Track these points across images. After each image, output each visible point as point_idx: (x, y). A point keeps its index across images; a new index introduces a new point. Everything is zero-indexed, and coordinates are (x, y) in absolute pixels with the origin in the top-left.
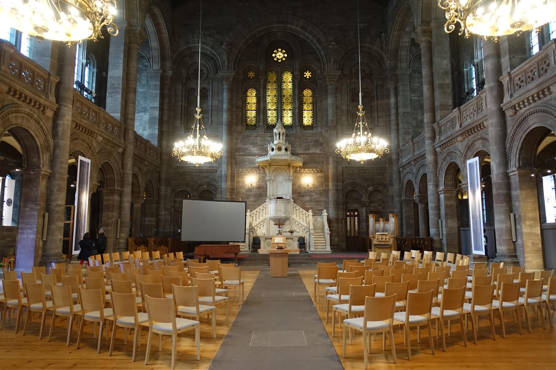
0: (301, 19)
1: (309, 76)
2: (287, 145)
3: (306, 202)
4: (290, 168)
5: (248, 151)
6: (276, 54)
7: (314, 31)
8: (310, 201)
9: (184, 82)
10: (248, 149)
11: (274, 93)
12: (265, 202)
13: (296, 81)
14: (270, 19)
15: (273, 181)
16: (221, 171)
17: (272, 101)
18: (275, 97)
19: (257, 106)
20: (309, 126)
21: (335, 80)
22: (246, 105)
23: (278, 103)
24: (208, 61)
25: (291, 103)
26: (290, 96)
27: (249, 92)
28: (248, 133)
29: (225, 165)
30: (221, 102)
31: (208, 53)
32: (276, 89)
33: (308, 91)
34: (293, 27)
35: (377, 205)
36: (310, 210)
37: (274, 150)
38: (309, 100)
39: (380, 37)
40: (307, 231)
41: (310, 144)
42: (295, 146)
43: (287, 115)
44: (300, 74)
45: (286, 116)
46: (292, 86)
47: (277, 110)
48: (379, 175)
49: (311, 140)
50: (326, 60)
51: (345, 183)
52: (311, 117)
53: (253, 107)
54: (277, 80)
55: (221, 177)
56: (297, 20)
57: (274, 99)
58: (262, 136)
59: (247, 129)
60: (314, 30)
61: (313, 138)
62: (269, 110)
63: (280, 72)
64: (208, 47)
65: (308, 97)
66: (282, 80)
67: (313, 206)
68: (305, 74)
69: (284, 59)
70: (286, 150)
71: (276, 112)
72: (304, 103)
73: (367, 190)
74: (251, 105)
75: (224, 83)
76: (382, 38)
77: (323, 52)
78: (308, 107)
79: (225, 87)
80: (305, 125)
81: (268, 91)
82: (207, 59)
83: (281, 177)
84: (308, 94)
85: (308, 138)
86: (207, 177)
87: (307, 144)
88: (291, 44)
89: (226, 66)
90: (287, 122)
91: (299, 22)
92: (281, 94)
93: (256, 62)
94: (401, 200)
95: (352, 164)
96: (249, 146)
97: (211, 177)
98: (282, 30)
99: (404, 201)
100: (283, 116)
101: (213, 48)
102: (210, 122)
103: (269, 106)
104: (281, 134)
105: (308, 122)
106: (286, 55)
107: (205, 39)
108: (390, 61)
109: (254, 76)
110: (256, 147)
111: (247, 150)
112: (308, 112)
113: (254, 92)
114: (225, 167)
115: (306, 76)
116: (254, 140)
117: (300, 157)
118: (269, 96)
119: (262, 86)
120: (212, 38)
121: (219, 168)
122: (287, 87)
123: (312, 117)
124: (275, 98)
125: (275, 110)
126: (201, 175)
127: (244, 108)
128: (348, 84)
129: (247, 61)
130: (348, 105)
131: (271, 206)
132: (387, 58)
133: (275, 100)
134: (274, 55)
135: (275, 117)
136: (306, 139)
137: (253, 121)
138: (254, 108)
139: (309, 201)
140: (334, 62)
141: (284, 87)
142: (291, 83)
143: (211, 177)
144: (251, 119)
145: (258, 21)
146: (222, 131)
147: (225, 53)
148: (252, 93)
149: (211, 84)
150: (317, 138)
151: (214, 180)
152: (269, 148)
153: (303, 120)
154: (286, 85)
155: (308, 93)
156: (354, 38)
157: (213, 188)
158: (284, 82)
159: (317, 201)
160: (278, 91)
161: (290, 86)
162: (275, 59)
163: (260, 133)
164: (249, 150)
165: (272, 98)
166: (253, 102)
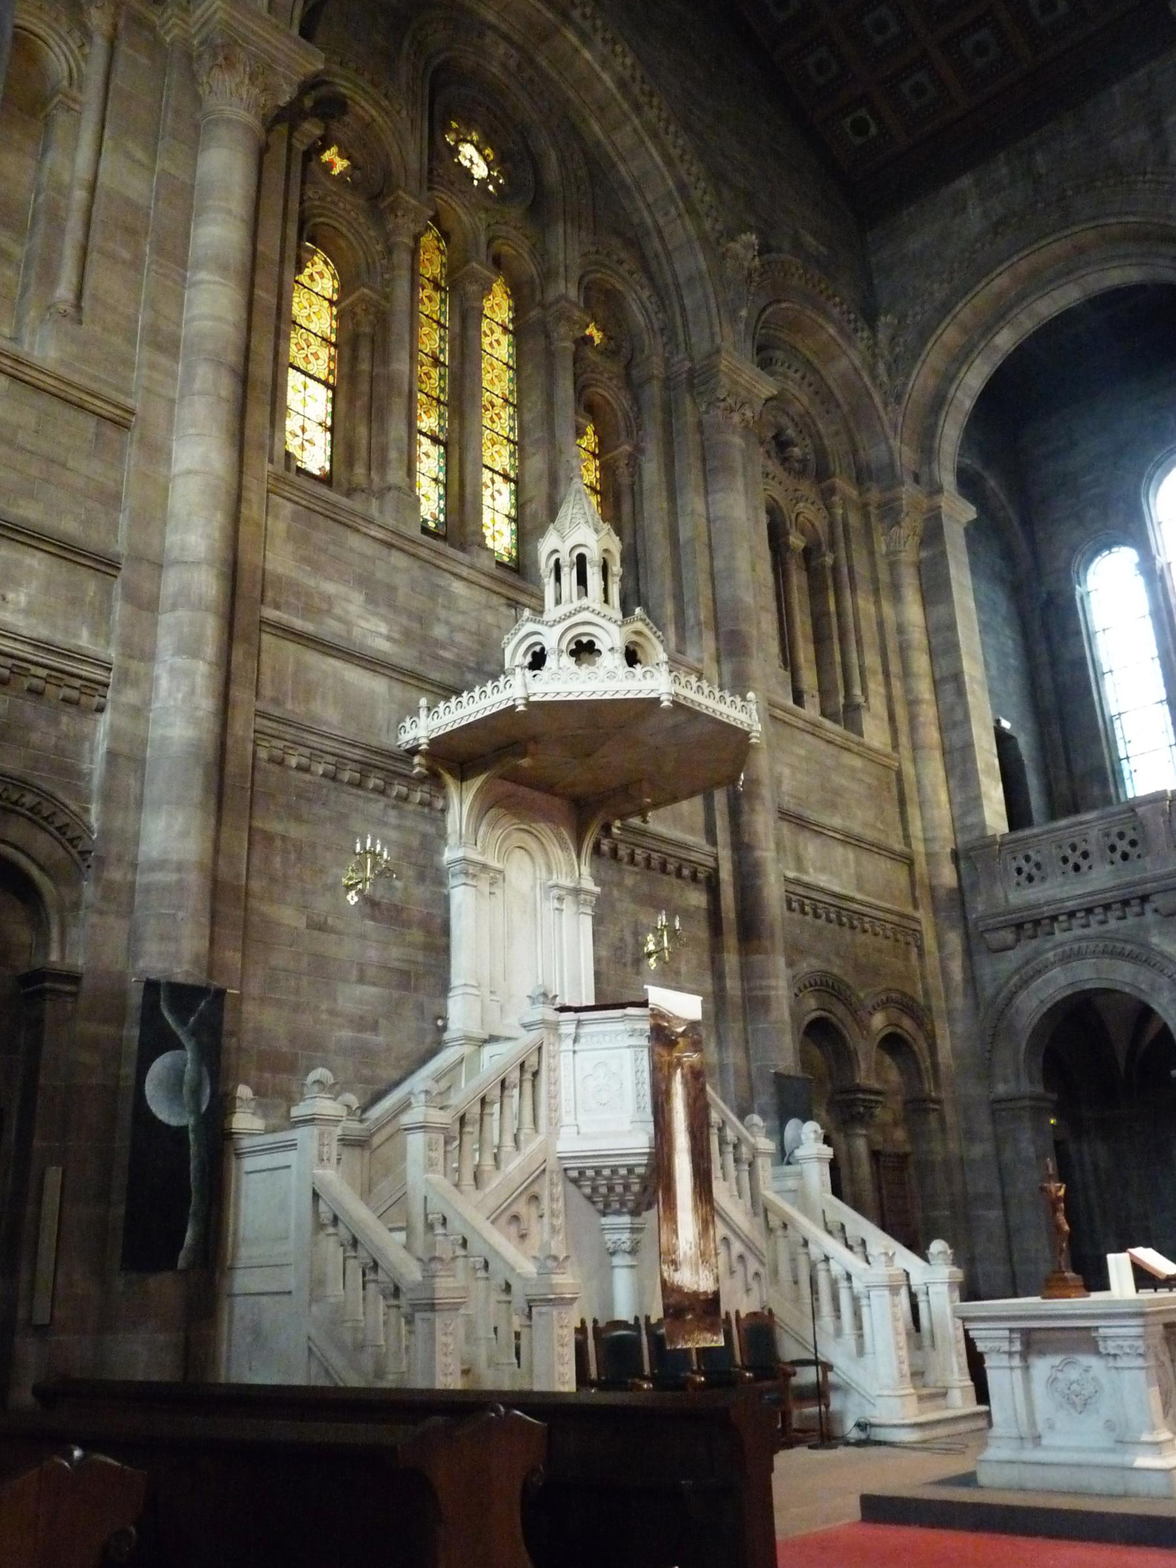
4: (482, 819)
10: (337, 610)
21: (749, 414)
37: (550, 662)
47: (445, 445)
94: (992, 1096)
95: (811, 870)
99: (1027, 1103)
110: (383, 610)
113: (327, 274)
121: (126, 678)
124: (435, 373)
138: (321, 365)
151: (71, 774)
157: (43, 843)
164: (339, 619)
166: (312, 327)
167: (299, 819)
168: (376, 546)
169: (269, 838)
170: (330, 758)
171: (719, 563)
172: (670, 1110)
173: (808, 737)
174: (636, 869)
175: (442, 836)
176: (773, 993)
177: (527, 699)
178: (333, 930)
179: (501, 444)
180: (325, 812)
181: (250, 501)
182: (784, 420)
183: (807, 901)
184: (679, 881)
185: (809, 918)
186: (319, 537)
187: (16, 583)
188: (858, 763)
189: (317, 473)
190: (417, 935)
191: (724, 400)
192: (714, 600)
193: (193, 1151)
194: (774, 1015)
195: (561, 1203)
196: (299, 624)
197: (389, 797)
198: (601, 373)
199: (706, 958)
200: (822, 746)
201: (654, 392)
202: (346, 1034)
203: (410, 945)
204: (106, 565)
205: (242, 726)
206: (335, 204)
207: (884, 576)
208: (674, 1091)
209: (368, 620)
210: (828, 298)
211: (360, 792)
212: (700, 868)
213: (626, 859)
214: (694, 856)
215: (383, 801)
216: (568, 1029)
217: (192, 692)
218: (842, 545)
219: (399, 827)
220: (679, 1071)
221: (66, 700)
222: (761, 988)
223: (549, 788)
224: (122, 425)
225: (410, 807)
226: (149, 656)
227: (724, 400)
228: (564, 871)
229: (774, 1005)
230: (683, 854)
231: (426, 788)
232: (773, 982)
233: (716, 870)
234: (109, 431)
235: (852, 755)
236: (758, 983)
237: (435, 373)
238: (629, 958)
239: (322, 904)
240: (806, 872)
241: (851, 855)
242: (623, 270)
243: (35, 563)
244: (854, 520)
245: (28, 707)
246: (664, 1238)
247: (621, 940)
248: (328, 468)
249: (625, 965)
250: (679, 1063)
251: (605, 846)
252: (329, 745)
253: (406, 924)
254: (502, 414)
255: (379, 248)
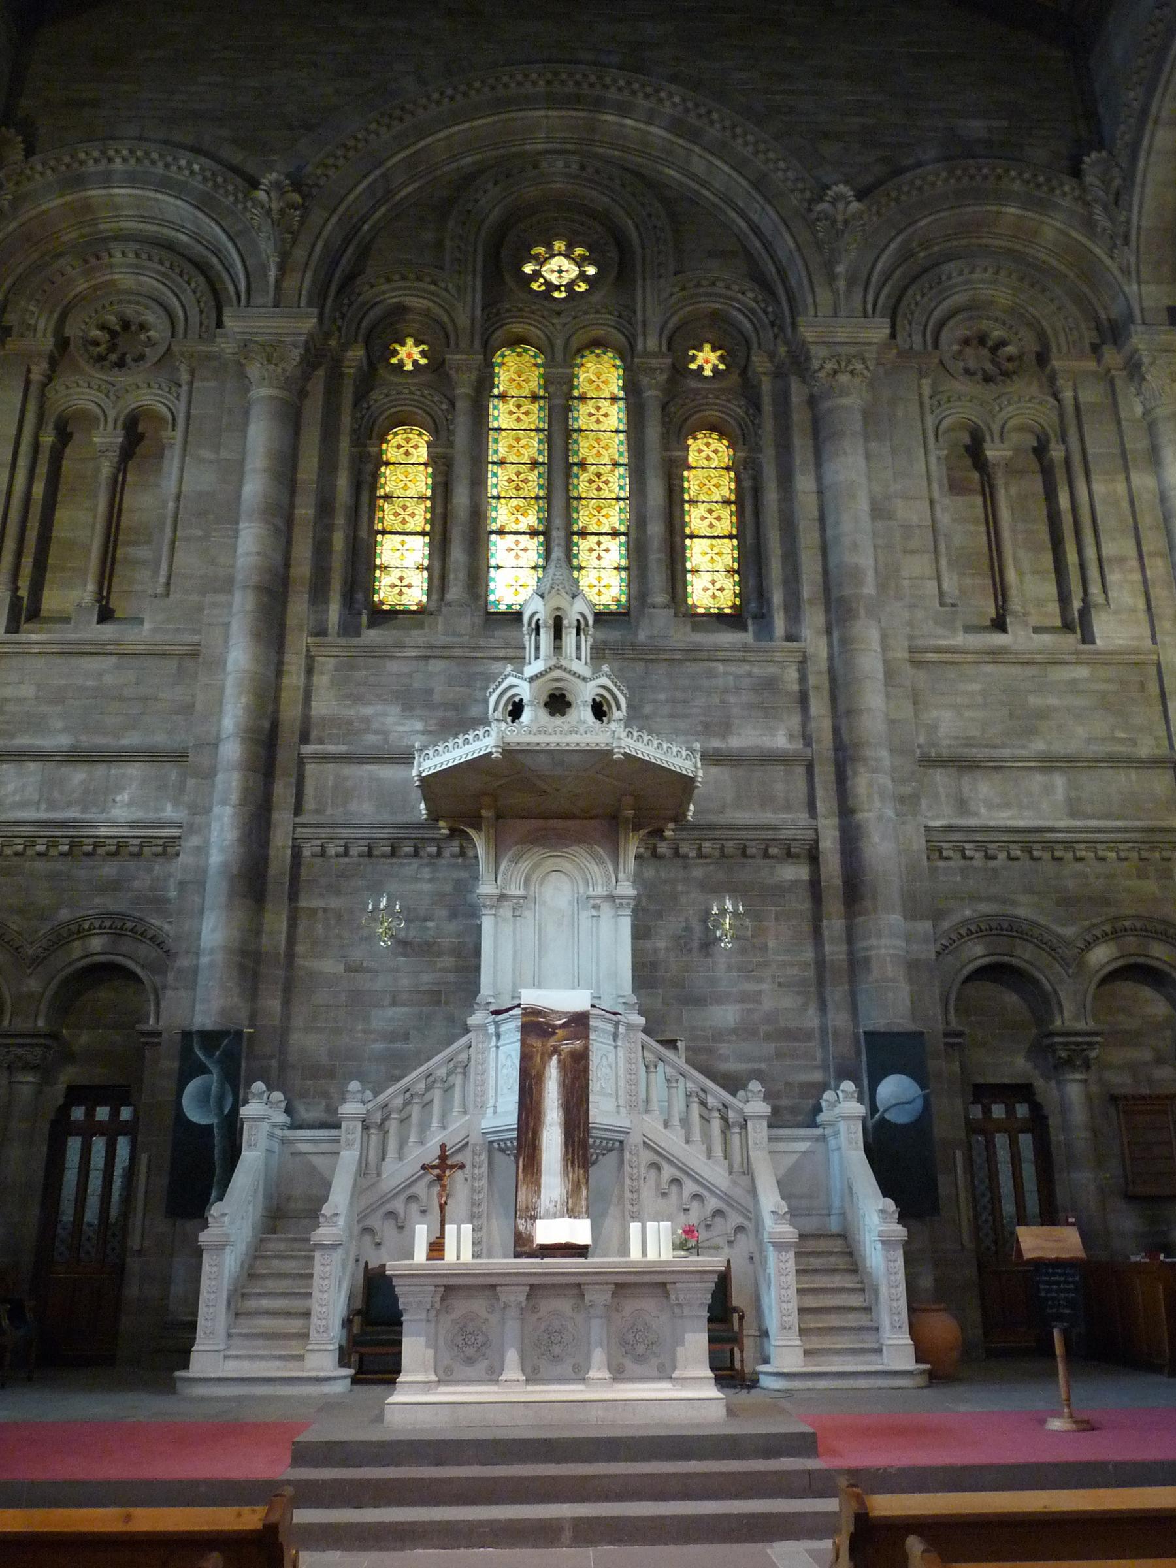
0: (673, 87)
1: (715, 369)
2: (604, 681)
3: (718, 1036)
5: (371, 739)
6: (542, 264)
7: (740, 141)
8: (746, 1031)
9: (36, 376)
10: (375, 726)
11: (532, 447)
12: (467, 1030)
13: (645, 380)
14: (513, 85)
15: (518, 907)
16: (202, 850)
17: (518, 488)
18: (532, 470)
19: (432, 510)
20: (720, 617)
22: (372, 509)
23: (548, 498)
24: (181, 275)
25: (618, 499)
26: (615, 464)
27: (394, 442)
28: (372, 636)
29: (228, 810)
30: (235, 471)
31: (184, 238)
32: (537, 430)
33: (708, 445)
34: (629, 122)
35: (1147, 1055)
36: (755, 1086)
38: (717, 486)
39: (1076, 173)
40: (740, 1229)
41: (732, 699)
42: (648, 709)
43: (599, 558)
44: (669, 349)
45: (596, 563)
46: (622, 415)
48: (1142, 875)
49: (737, 677)
50: (807, 269)
51: (946, 925)
52: (730, 572)
53: (412, 515)
54: (546, 387)
55: (202, 884)
56: (649, 90)
57: (525, 481)
58: (457, 652)
59: (372, 624)
60: (734, 136)
61: (746, 667)
62: (501, 532)
63: (559, 343)
64: (179, 202)
65: (713, 473)
66: (572, 387)
67: (763, 1066)
68: (694, 358)
69: (582, 287)
70: (599, 710)
71: (540, 544)
72: (690, 502)
73: (1081, 964)
74: (405, 508)
75: (254, 370)
76: (1089, 179)
77: (787, 236)
78: (710, 519)
79: (261, 392)
80: (701, 611)
81: (496, 441)
82: (171, 268)
83: (566, 886)
84: (708, 458)
85: (720, 667)
86: (114, 886)
87: (716, 700)
88: (622, 213)
89: (272, 289)
90: (599, 593)
91: (661, 101)
92: (567, 457)
93: (432, 288)
95: (983, 811)
96: (379, 707)
97: (136, 884)
98: (569, 147)
100: (575, 562)
101: (205, 204)
102: (162, 580)
103: (501, 515)
104: (565, 622)
105: (714, 597)
106: (591, 271)
107: (167, 166)
108: (1139, 283)
109: (423, 361)
110: (419, 712)
111: (367, 730)
112: (712, 547)
114: (226, 820)
115: (701, 368)
116: (410, 675)
117: (684, 753)
118: (501, 463)
119: (462, 405)
120: (203, 160)
121: (192, 829)
122: (598, 421)
123: (737, 572)
124: (533, 476)
125: (533, 533)
126: (82, 873)
127: (365, 518)
128: (927, 401)
129: (388, 280)
130: (932, 502)
131: (502, 1056)
132: (1126, 272)
133: (534, 483)
134: (528, 269)
135: (535, 568)
136: (711, 674)
137: (409, 586)
138: (419, 517)
139: (735, 1031)
140: (851, 282)
141: (582, 423)
142: (621, 404)
143: (136, 884)
144: (401, 579)
145: (449, 92)
146: (227, 625)
147: (267, 227)
148: (408, 447)
149: (185, 388)
150: (773, 670)
151: (159, 903)
152: (492, 701)
153: (685, 583)
154: (591, 415)
155: (708, 452)
156: (944, 174)
157: (145, 950)
158: (583, 398)
159: (789, 1035)
160: (550, 439)
161: (615, 416)
162: (534, 286)
163: (442, 640)
164: (377, 733)
165: (518, 474)
166: (409, 493)
167: (338, 893)
168: (415, 662)
169: (313, 912)
170: (362, 842)
171: (830, 533)
172: (540, 1092)
173: (989, 668)
174: (708, 861)
175: (476, 878)
176: (873, 953)
177: (419, 776)
178: (368, 970)
179: (610, 506)
180: (360, 883)
181: (289, 672)
182: (985, 325)
183: (967, 846)
184: (769, 861)
185: (979, 860)
186: (360, 675)
187: (120, 788)
188: (1083, 672)
189: (415, 608)
190: (448, 961)
191: (822, 368)
192: (826, 572)
193: (217, 1140)
194: (875, 974)
195: (484, 1169)
196: (332, 749)
197: (422, 858)
198: (706, 397)
199: (806, 926)
200: (1014, 670)
201: (766, 386)
202: (379, 1046)
203: (444, 970)
204: (179, 756)
205: (281, 840)
206: (399, 393)
207: (1137, 443)
208: (547, 1074)
209: (403, 724)
210: (999, 178)
211: (395, 861)
212: (793, 844)
213: (692, 854)
214: (783, 834)
215: (415, 863)
216: (491, 1029)
217: (222, 830)
218: (1072, 432)
219: (431, 880)
220: (555, 1058)
221: (156, 855)
222: (864, 948)
223: (587, 816)
224: (194, 655)
225: (444, 861)
226: (207, 810)
227: (822, 368)
228: (600, 881)
229: (874, 965)
230: (770, 835)
231: (456, 843)
232: (873, 942)
233: (817, 841)
234: (188, 663)
235: (1072, 667)
236: (865, 944)
237: (533, 476)
238: (695, 944)
239: (357, 954)
240: (976, 814)
241: (1059, 781)
242: (720, 288)
243: (134, 772)
244: (1091, 395)
245: (132, 865)
246: (522, 1198)
247: (688, 929)
248: (424, 599)
249: (690, 951)
250: (556, 1050)
251: (663, 848)
252: (359, 833)
253: (439, 954)
254: (610, 479)
255: (444, 407)
